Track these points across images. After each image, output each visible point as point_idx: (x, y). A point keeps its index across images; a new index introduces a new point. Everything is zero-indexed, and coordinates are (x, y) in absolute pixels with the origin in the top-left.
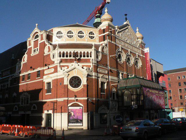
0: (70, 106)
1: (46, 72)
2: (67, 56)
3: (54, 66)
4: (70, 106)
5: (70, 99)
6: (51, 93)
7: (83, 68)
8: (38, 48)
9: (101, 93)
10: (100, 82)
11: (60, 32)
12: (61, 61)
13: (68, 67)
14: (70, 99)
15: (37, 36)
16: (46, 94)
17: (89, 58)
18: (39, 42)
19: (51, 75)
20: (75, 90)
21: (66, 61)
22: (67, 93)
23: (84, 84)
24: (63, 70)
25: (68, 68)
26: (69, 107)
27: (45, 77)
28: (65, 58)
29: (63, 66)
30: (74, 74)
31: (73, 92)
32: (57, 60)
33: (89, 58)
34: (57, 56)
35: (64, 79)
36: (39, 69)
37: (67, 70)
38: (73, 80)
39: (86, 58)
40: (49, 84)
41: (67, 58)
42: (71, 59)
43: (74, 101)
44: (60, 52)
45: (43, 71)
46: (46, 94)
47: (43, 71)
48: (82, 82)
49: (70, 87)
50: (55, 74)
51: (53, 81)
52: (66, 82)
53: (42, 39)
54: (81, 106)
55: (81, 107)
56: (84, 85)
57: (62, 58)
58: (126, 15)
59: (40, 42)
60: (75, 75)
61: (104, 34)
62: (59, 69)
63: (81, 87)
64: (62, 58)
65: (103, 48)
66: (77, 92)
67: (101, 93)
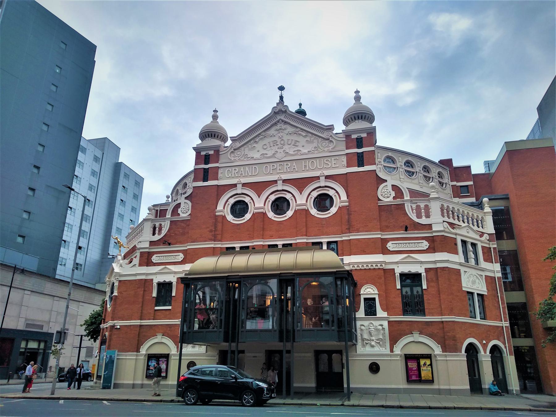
9: (157, 308)
58: (281, 88)
67: (157, 308)
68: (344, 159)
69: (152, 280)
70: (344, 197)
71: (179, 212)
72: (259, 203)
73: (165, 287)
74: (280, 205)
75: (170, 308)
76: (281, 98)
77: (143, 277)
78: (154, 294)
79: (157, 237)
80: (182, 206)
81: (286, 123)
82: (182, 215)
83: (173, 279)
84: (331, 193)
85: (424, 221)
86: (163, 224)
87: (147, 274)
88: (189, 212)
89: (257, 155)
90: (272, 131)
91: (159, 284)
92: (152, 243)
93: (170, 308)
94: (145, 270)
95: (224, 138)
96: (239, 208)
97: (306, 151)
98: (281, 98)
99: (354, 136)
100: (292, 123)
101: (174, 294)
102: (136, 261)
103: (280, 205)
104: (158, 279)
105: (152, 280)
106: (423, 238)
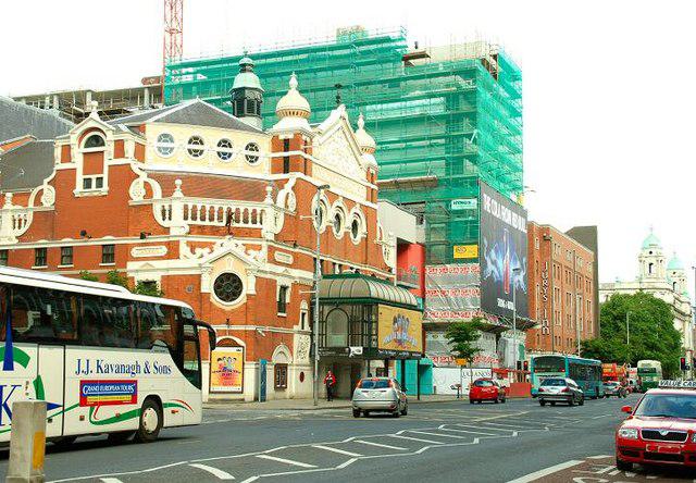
1: (135, 252)
2: (203, 219)
3: (166, 240)
11: (166, 135)
12: (193, 230)
13: (210, 245)
17: (258, 226)
20: (228, 306)
21: (202, 230)
24: (198, 255)
27: (131, 265)
29: (202, 245)
30: (229, 267)
31: (223, 311)
32: (178, 226)
33: (258, 226)
34: (178, 213)
35: (203, 278)
36: (108, 240)
38: (222, 281)
39: (250, 225)
42: (213, 227)
45: (127, 248)
49: (215, 299)
52: (207, 286)
56: (248, 296)
57: (190, 221)
59: (109, 160)
60: (229, 269)
62: (184, 249)
63: (242, 299)
66: (233, 312)
75: (284, 315)
77: (268, 276)
84: (359, 221)
87: (274, 274)
93: (284, 315)
102: (264, 252)
104: (281, 281)
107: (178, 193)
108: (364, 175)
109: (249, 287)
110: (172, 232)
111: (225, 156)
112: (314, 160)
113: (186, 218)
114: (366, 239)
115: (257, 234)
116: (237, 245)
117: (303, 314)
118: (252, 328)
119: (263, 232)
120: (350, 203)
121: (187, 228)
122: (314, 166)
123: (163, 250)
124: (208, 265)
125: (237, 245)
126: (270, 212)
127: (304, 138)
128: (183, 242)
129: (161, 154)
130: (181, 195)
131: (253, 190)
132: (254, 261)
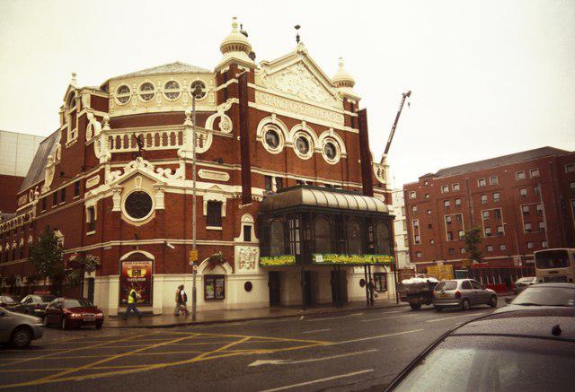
0: (124, 260)
1: (88, 185)
3: (99, 170)
4: (125, 260)
5: (125, 243)
6: (94, 232)
7: (156, 172)
8: (77, 129)
9: (208, 228)
10: (205, 203)
12: (115, 157)
14: (125, 243)
15: (74, 104)
16: (88, 234)
18: (78, 116)
19: (94, 192)
22: (121, 229)
23: (157, 208)
25: (123, 173)
26: (124, 263)
28: (122, 150)
30: (138, 185)
37: (118, 178)
39: (169, 147)
40: (91, 209)
41: (126, 150)
43: (134, 248)
44: (111, 138)
45: (85, 180)
46: (88, 234)
47: (85, 180)
48: (153, 203)
49: (126, 216)
50: (103, 188)
51: (99, 202)
52: (119, 205)
53: (82, 109)
54: (151, 260)
55: (151, 263)
56: (157, 211)
58: (297, 27)
61: (225, 86)
63: (150, 216)
64: (115, 150)
65: (218, 120)
67: (208, 228)
68: (343, 117)
69: (201, 197)
70: (344, 151)
71: (220, 125)
72: (290, 137)
73: (215, 206)
74: (304, 143)
76: (298, 37)
78: (205, 213)
79: (200, 151)
80: (223, 120)
81: (305, 66)
82: (223, 131)
83: (223, 199)
84: (335, 144)
85: (382, 181)
86: (205, 136)
88: (229, 131)
89: (285, 90)
90: (294, 69)
91: (210, 203)
92: (199, 157)
94: (190, 184)
95: (252, 56)
96: (273, 137)
97: (319, 100)
98: (298, 37)
99: (349, 101)
100: (310, 68)
101: (224, 214)
102: (181, 171)
103: (304, 143)
104: (208, 197)
105: (201, 197)
106: (382, 193)
107: (107, 128)
108: (340, 104)
109: (158, 203)
110: (102, 161)
111: (172, 95)
112: (257, 88)
113: (112, 148)
114: (347, 159)
115: (173, 154)
116: (146, 165)
117: (247, 229)
118: (160, 241)
119: (179, 152)
120: (319, 129)
121: (109, 156)
122: (257, 94)
123: (97, 180)
124: (117, 185)
125: (146, 165)
126: (189, 135)
127: (240, 67)
128: (108, 167)
129: (144, 101)
130: (109, 129)
131: (177, 118)
132: (164, 180)
